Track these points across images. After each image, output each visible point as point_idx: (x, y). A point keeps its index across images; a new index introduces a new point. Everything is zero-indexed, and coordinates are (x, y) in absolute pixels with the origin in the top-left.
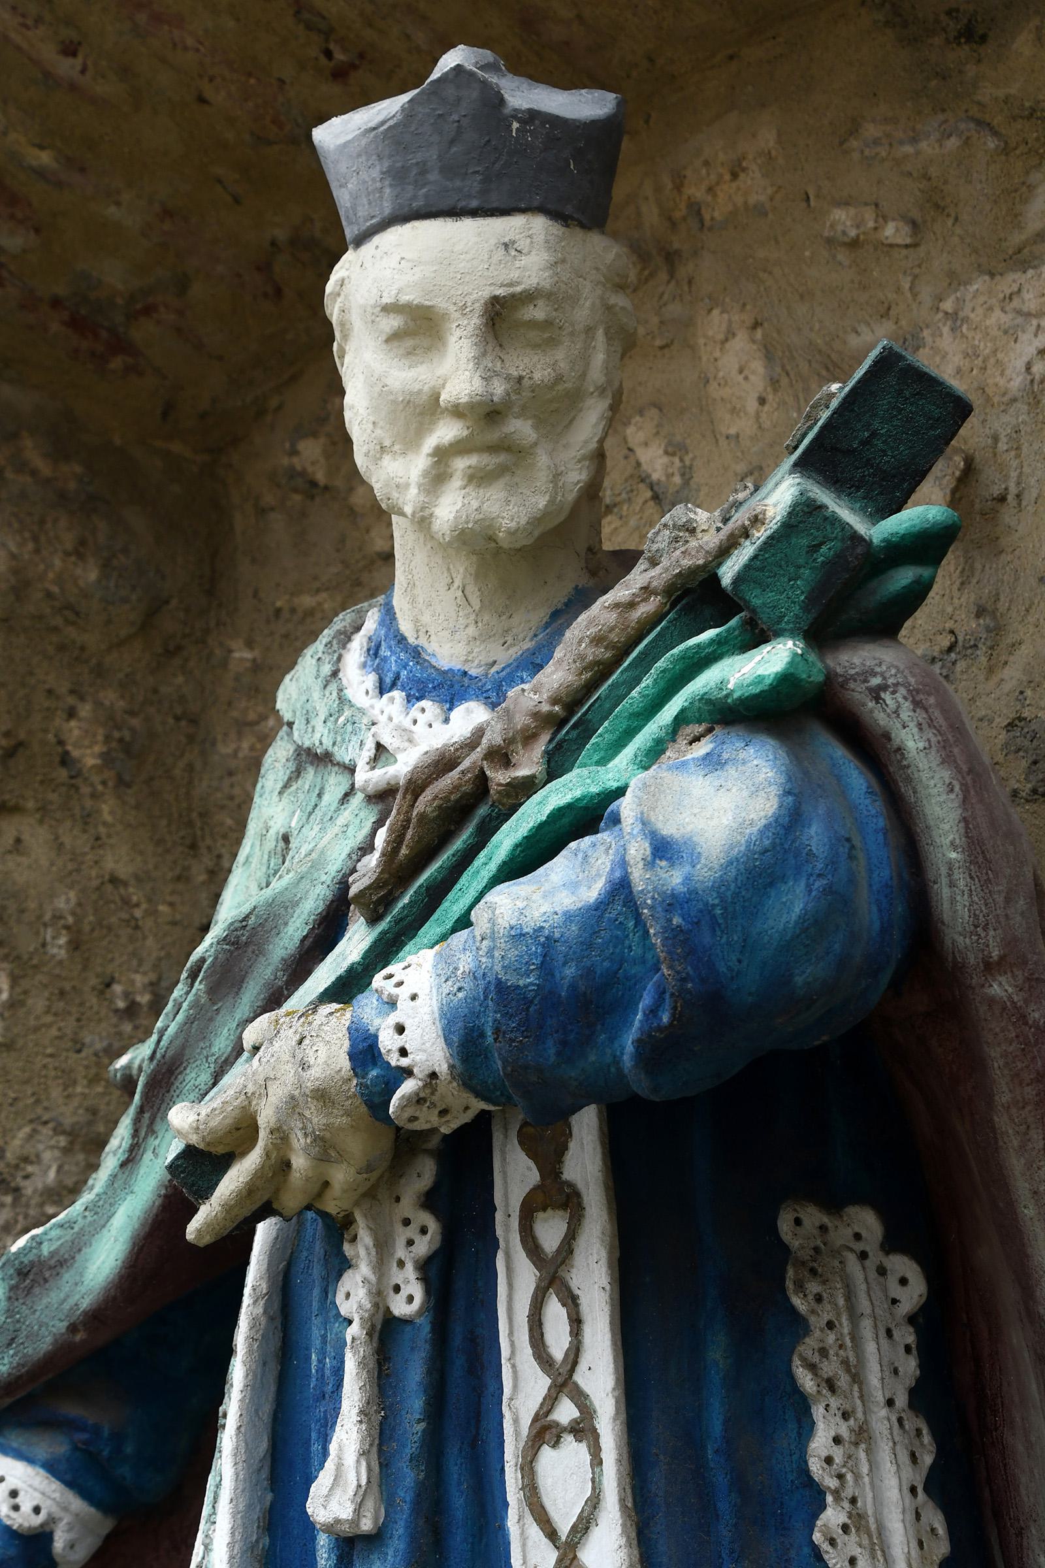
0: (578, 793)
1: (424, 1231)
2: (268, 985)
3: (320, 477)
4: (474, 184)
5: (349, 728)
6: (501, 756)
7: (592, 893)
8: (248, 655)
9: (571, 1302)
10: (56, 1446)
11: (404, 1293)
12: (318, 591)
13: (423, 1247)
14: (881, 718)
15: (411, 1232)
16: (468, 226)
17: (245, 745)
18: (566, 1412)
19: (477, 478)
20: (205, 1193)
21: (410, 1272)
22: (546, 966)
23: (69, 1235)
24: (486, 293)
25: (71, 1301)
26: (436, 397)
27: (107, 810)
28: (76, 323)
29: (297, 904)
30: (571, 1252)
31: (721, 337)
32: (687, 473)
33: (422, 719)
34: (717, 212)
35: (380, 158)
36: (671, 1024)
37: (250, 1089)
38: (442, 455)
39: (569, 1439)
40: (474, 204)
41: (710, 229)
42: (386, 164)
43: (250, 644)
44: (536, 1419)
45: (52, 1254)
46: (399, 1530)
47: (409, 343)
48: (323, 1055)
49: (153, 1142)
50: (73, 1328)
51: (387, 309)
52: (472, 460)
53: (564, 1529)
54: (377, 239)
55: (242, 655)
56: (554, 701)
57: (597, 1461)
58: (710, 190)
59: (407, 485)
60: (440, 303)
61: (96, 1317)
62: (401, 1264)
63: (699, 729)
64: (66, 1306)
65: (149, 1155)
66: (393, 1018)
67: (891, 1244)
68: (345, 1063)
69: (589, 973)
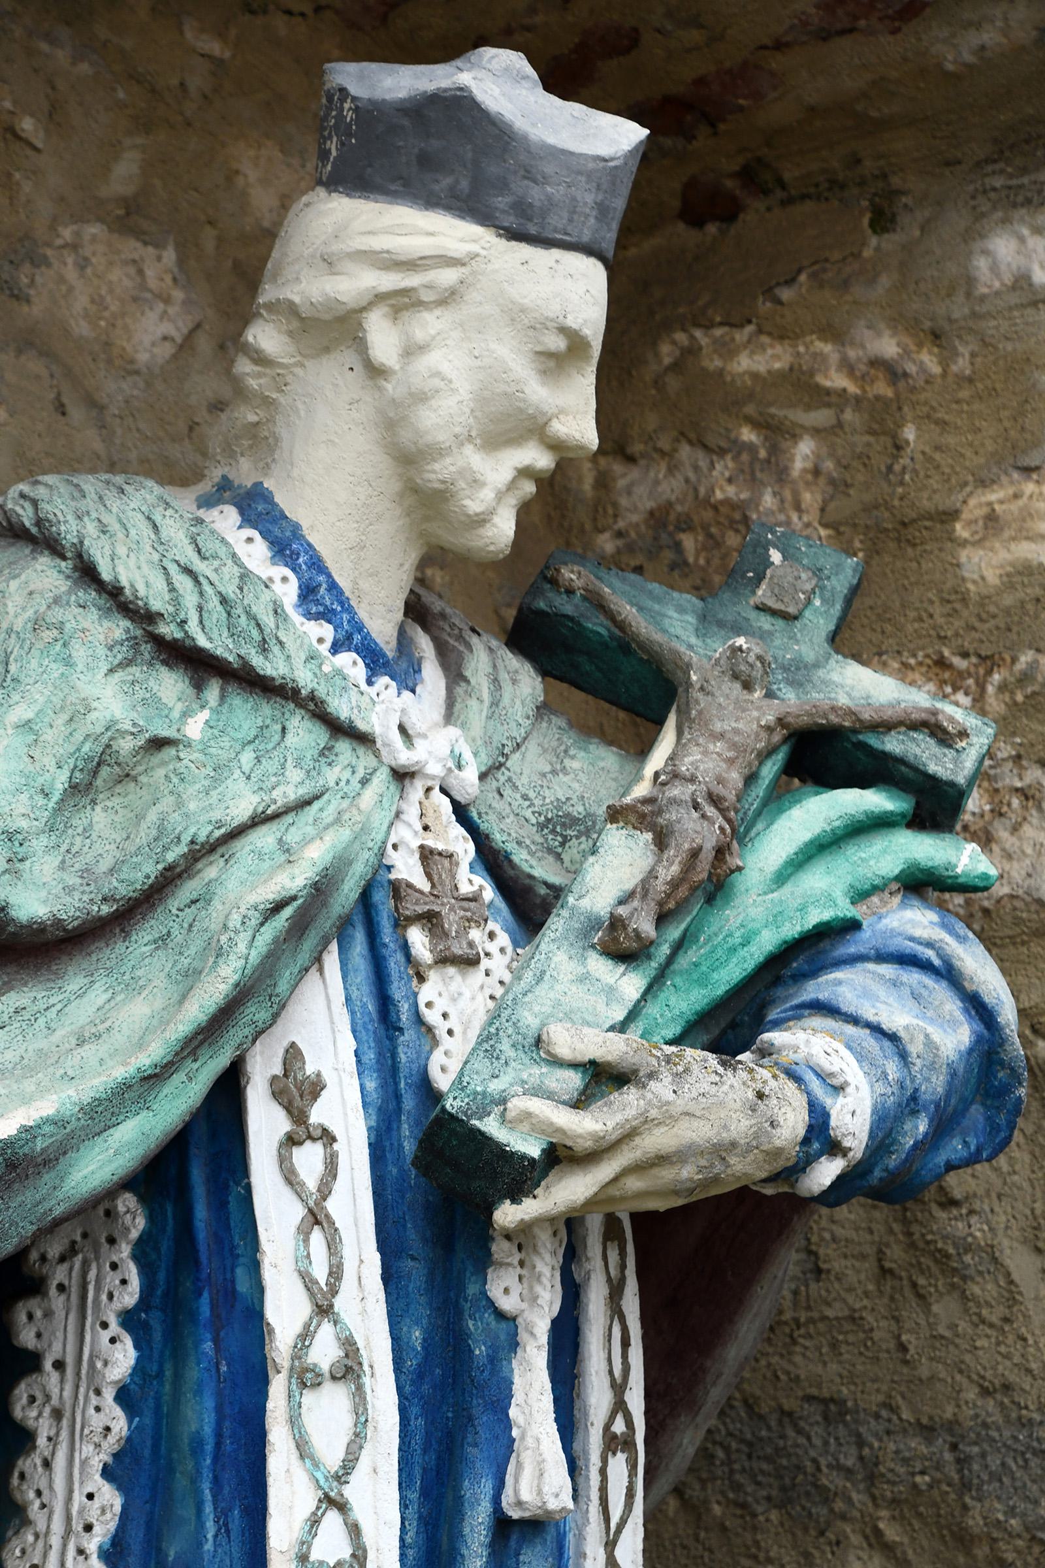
25: (47, 1205)
35: (598, 187)
37: (654, 1113)
54: (556, 253)
64: (41, 1209)
65: (179, 1078)
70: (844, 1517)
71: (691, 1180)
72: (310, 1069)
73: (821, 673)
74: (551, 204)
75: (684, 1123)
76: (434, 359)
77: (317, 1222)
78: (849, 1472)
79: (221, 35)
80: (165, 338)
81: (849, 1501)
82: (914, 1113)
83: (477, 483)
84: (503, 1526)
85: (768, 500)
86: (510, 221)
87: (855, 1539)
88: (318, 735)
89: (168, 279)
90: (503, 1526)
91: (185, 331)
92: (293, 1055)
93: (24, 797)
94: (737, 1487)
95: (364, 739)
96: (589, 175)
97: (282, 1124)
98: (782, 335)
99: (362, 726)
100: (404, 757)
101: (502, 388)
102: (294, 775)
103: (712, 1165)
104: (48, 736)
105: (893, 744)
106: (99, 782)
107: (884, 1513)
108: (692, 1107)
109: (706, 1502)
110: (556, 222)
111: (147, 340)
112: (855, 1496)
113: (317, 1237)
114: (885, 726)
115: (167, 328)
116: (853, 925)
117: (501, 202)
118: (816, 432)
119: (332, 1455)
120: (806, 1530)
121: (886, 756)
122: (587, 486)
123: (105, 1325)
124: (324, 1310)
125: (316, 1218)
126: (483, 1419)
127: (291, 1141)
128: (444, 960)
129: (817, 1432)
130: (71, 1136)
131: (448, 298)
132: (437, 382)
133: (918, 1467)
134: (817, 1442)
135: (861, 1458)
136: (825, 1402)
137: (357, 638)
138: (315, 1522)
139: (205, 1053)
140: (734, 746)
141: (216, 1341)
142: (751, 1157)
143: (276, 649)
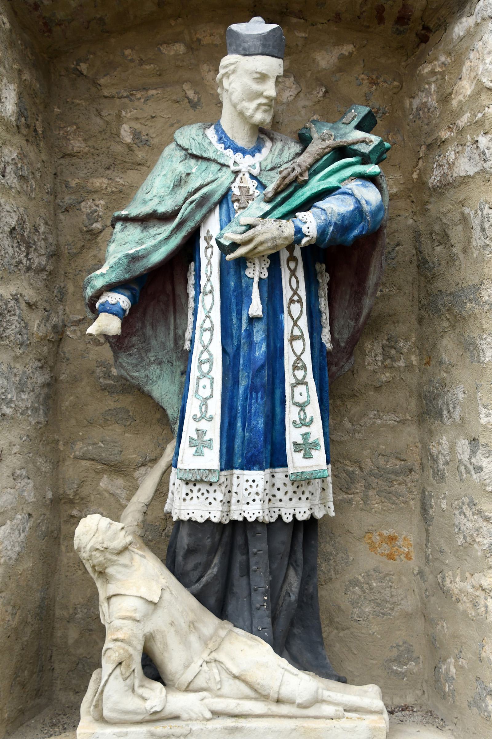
0: (328, 186)
1: (268, 262)
2: (210, 207)
3: (85, 73)
4: (276, 51)
5: (221, 155)
6: (301, 174)
7: (352, 208)
8: (59, 110)
9: (296, 278)
10: (128, 293)
11: (263, 273)
12: (81, 100)
13: (268, 265)
14: (381, 181)
15: (265, 262)
16: (274, 59)
17: (61, 133)
18: (296, 298)
19: (265, 111)
20: (232, 252)
21: (265, 270)
22: (343, 221)
23: (146, 252)
24: (277, 74)
25: (146, 265)
26: (262, 93)
27: (42, 144)
28: (45, 24)
29: (217, 192)
31: (207, 71)
32: (199, 99)
33: (239, 157)
34: (204, 42)
35: (260, 41)
36: (365, 234)
37: (257, 233)
38: (260, 105)
39: (296, 303)
40: (276, 55)
41: (203, 46)
42: (262, 42)
43: (59, 108)
44: (290, 299)
45: (142, 255)
46: (265, 317)
47: (259, 80)
48: (288, 230)
49: (175, 235)
50: (145, 271)
51: (257, 73)
52: (266, 107)
53: (295, 319)
54: (254, 57)
55: (57, 110)
56: (309, 165)
57: (302, 306)
58: (204, 37)
59: (249, 109)
60: (270, 74)
62: (263, 268)
63: (353, 178)
64: (144, 266)
65: (173, 238)
66: (307, 225)
67: (326, 271)
68: (293, 233)
69: (349, 222)
72: (210, 233)
73: (348, 135)
74: (250, 47)
76: (232, 85)
79: (305, 32)
80: (291, 96)
82: (331, 226)
83: (248, 109)
85: (430, 100)
86: (243, 52)
88: (219, 167)
89: (292, 84)
90: (252, 320)
91: (296, 93)
92: (208, 231)
93: (163, 189)
95: (228, 166)
96: (257, 38)
97: (206, 245)
98: (430, 62)
99: (226, 164)
100: (236, 168)
101: (247, 88)
102: (211, 176)
104: (169, 176)
105: (356, 147)
106: (182, 184)
108: (265, 231)
110: (252, 50)
111: (286, 97)
113: (209, 266)
114: (354, 144)
115: (291, 93)
116: (338, 188)
117: (241, 49)
118: (434, 82)
119: (208, 308)
121: (355, 150)
122: (408, 106)
124: (209, 280)
125: (209, 263)
127: (207, 248)
128: (239, 208)
130: (150, 251)
131: (234, 72)
132: (233, 90)
137: (232, 146)
138: (204, 320)
139: (178, 232)
140: (310, 154)
143: (207, 151)
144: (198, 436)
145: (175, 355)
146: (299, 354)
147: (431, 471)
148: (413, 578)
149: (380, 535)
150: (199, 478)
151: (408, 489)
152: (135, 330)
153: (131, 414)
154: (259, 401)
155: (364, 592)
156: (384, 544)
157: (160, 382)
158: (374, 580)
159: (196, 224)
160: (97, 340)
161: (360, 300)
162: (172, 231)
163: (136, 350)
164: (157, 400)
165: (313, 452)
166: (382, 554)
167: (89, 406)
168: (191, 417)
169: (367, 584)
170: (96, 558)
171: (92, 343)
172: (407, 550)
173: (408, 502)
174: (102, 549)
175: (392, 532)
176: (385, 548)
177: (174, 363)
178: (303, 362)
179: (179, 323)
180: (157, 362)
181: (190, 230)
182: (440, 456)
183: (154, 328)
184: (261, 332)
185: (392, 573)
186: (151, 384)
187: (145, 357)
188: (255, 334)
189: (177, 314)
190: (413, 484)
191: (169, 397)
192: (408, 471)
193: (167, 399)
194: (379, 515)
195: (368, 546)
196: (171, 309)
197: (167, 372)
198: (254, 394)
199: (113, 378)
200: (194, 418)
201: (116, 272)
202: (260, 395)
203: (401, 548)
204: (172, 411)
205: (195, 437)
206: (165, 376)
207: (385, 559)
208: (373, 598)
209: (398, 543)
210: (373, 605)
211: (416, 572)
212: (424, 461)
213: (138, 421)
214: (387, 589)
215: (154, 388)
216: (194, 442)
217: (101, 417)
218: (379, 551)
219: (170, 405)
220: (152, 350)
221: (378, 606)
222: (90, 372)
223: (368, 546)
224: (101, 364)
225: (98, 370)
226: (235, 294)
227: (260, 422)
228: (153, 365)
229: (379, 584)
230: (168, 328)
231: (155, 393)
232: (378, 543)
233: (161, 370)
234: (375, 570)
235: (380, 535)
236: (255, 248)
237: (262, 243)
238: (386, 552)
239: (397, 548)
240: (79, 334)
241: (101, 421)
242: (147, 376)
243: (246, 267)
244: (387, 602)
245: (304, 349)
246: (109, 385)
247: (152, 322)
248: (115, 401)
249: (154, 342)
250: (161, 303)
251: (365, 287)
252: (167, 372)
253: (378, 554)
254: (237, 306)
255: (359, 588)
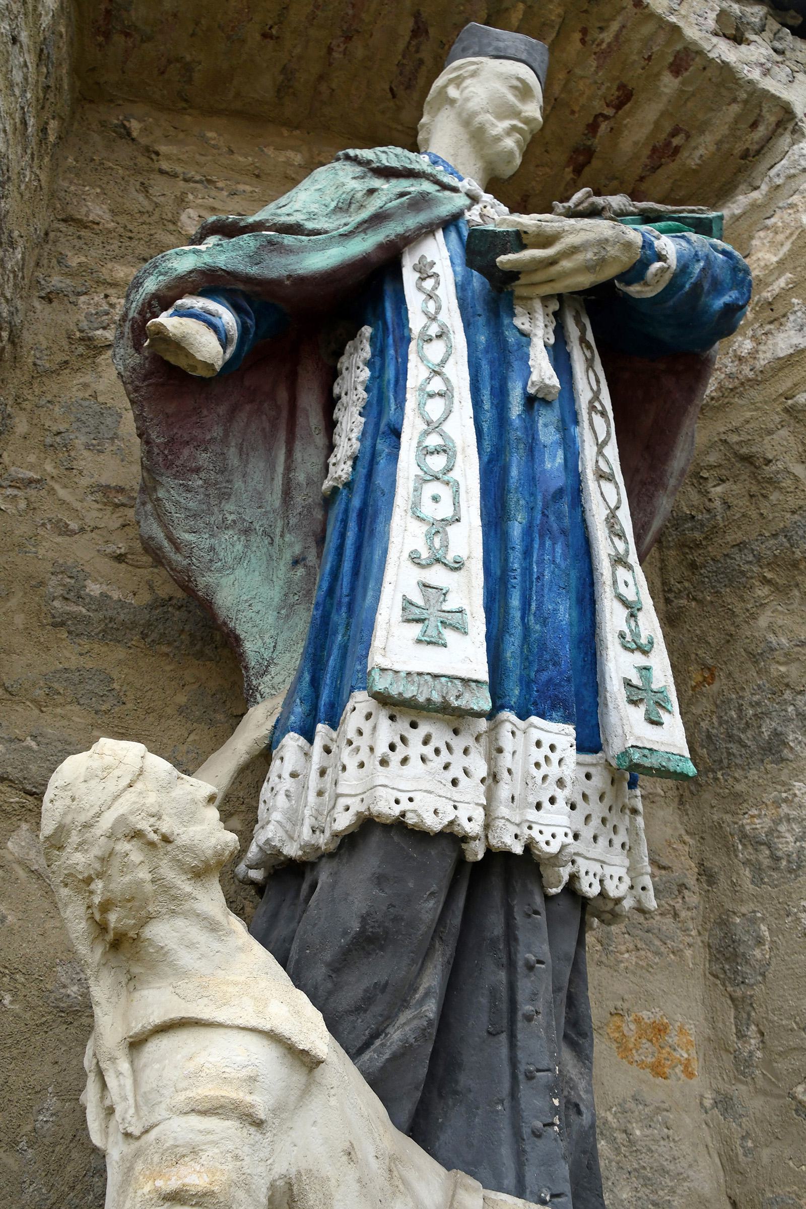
30: (383, 392)
37: (567, 228)
45: (288, 246)
49: (363, 235)
50: (289, 277)
61: (301, 281)
64: (290, 267)
70: (752, 578)
71: (592, 259)
75: (582, 233)
77: (431, 297)
78: (750, 562)
81: (753, 571)
82: (698, 261)
84: (531, 401)
87: (757, 583)
90: (531, 401)
94: (713, 587)
103: (600, 252)
107: (766, 570)
108: (584, 227)
109: (704, 598)
112: (754, 569)
120: (739, 589)
123: (358, 368)
126: (516, 365)
129: (737, 557)
133: (774, 548)
134: (738, 559)
135: (754, 556)
136: (738, 545)
141: (396, 351)
142: (617, 247)
144: (427, 601)
145: (280, 523)
146: (612, 506)
147: (747, 872)
148: (704, 1116)
149: (638, 1021)
150: (436, 697)
151: (680, 925)
152: (208, 437)
153: (116, 686)
154: (558, 561)
155: (617, 1151)
156: (644, 1041)
157: (240, 572)
158: (637, 1122)
159: (406, 232)
160: (61, 524)
161: (651, 497)
162: (360, 224)
163: (200, 482)
164: (222, 614)
165: (665, 717)
166: (642, 1065)
167: (14, 657)
168: (406, 555)
169: (625, 1131)
170: (126, 868)
171: (49, 527)
172: (686, 1056)
173: (681, 950)
174: (155, 838)
175: (658, 1016)
176: (646, 1052)
177: (277, 539)
178: (621, 525)
179: (299, 460)
180: (239, 525)
181: (392, 237)
182: (783, 828)
183: (244, 456)
184: (552, 429)
185: (666, 1106)
186: (219, 571)
187: (216, 509)
188: (540, 428)
189: (298, 445)
190: (689, 913)
191: (255, 609)
192: (675, 888)
193: (250, 614)
194: (632, 978)
195: (614, 1046)
196: (282, 435)
197: (258, 554)
198: (548, 543)
199: (87, 601)
200: (415, 559)
201: (228, 255)
202: (559, 549)
203: (675, 1050)
204: (260, 643)
205: (418, 599)
206: (254, 561)
207: (647, 1074)
208: (636, 1166)
209: (670, 1040)
210: (636, 1183)
211: (708, 1103)
212: (715, 863)
213: (130, 706)
214: (662, 1143)
215: (224, 581)
216: (417, 611)
217: (42, 683)
218: (637, 1058)
219: (255, 630)
220: (233, 498)
221: (646, 1185)
222: (33, 583)
223: (614, 1046)
224: (60, 570)
225: (54, 581)
226: (489, 356)
227: (561, 608)
228: (231, 532)
229: (648, 1132)
230: (272, 467)
231: (224, 594)
232: (633, 1040)
233: (246, 547)
234: (635, 1099)
235: (638, 1021)
236: (552, 262)
237: (573, 250)
238: (650, 1060)
239: (668, 1049)
240: (22, 505)
241: (38, 692)
242: (212, 549)
243: (513, 315)
244: (664, 1171)
245: (619, 501)
246: (74, 617)
247: (242, 444)
248: (81, 655)
249: (238, 484)
250: (264, 417)
251: (666, 471)
252: (258, 554)
253: (635, 1064)
254: (491, 379)
255: (607, 1142)
